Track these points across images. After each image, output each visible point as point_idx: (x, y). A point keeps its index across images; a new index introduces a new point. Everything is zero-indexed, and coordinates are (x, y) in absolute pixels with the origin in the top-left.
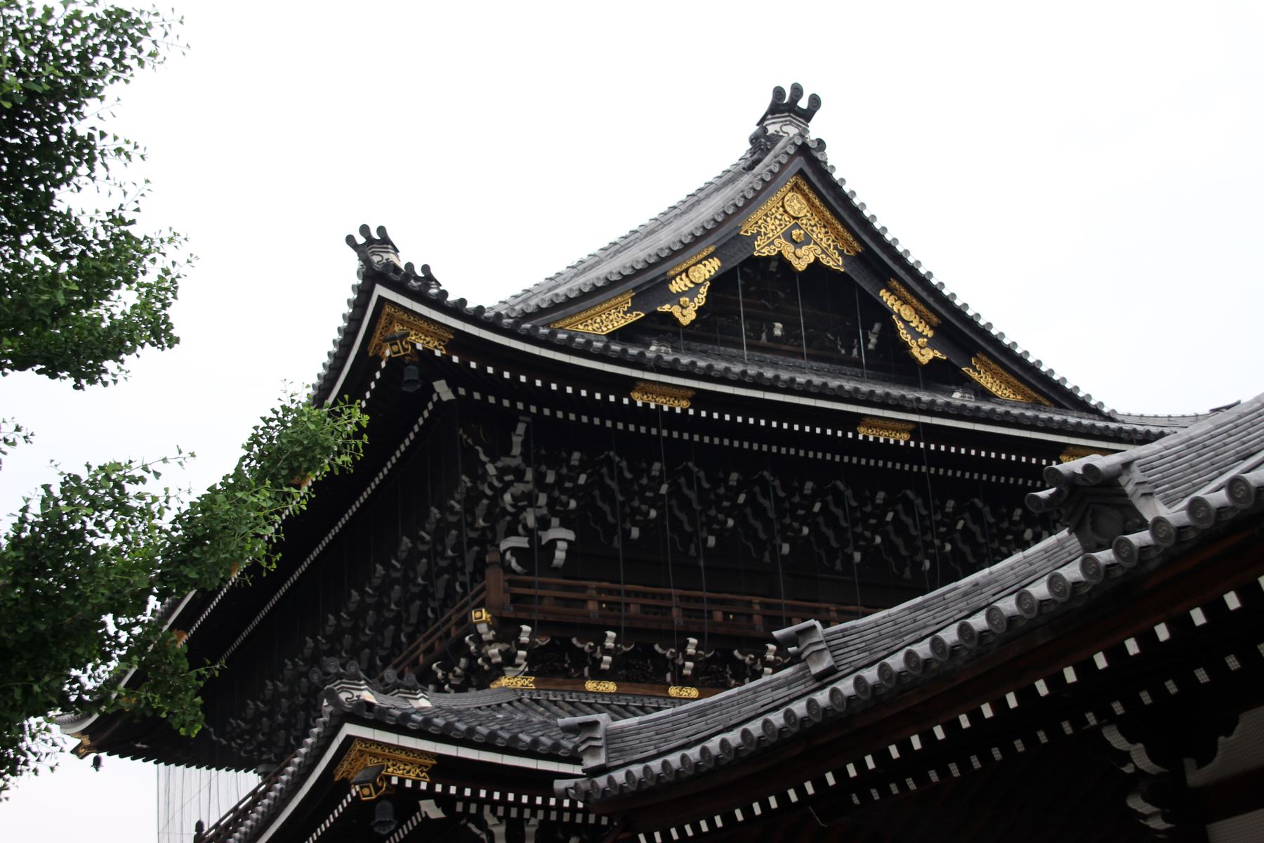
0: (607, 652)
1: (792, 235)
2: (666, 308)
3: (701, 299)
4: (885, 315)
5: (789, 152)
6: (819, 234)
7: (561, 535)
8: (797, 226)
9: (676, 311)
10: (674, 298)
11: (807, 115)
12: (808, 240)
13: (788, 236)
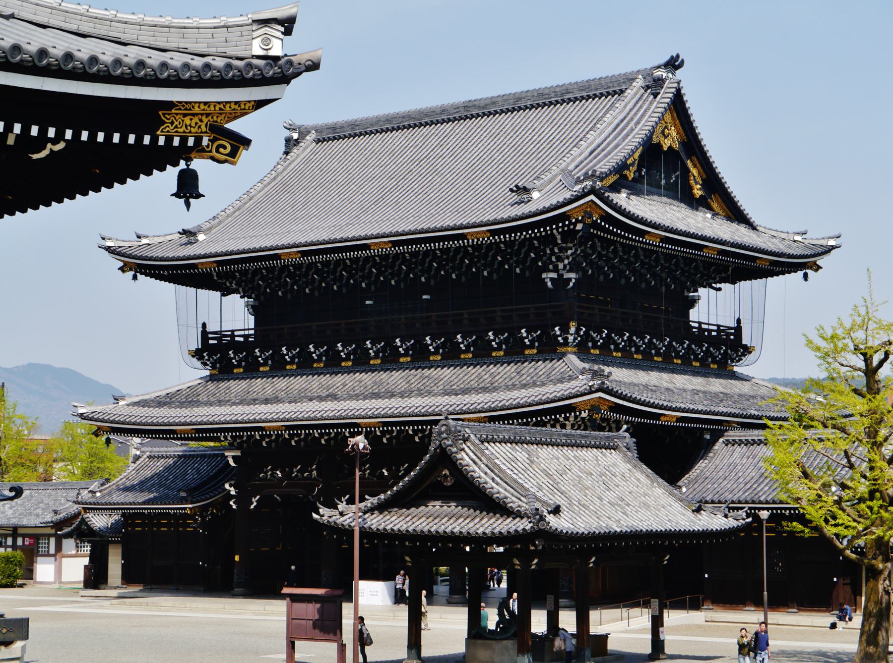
4: (686, 172)
6: (673, 132)
8: (666, 127)
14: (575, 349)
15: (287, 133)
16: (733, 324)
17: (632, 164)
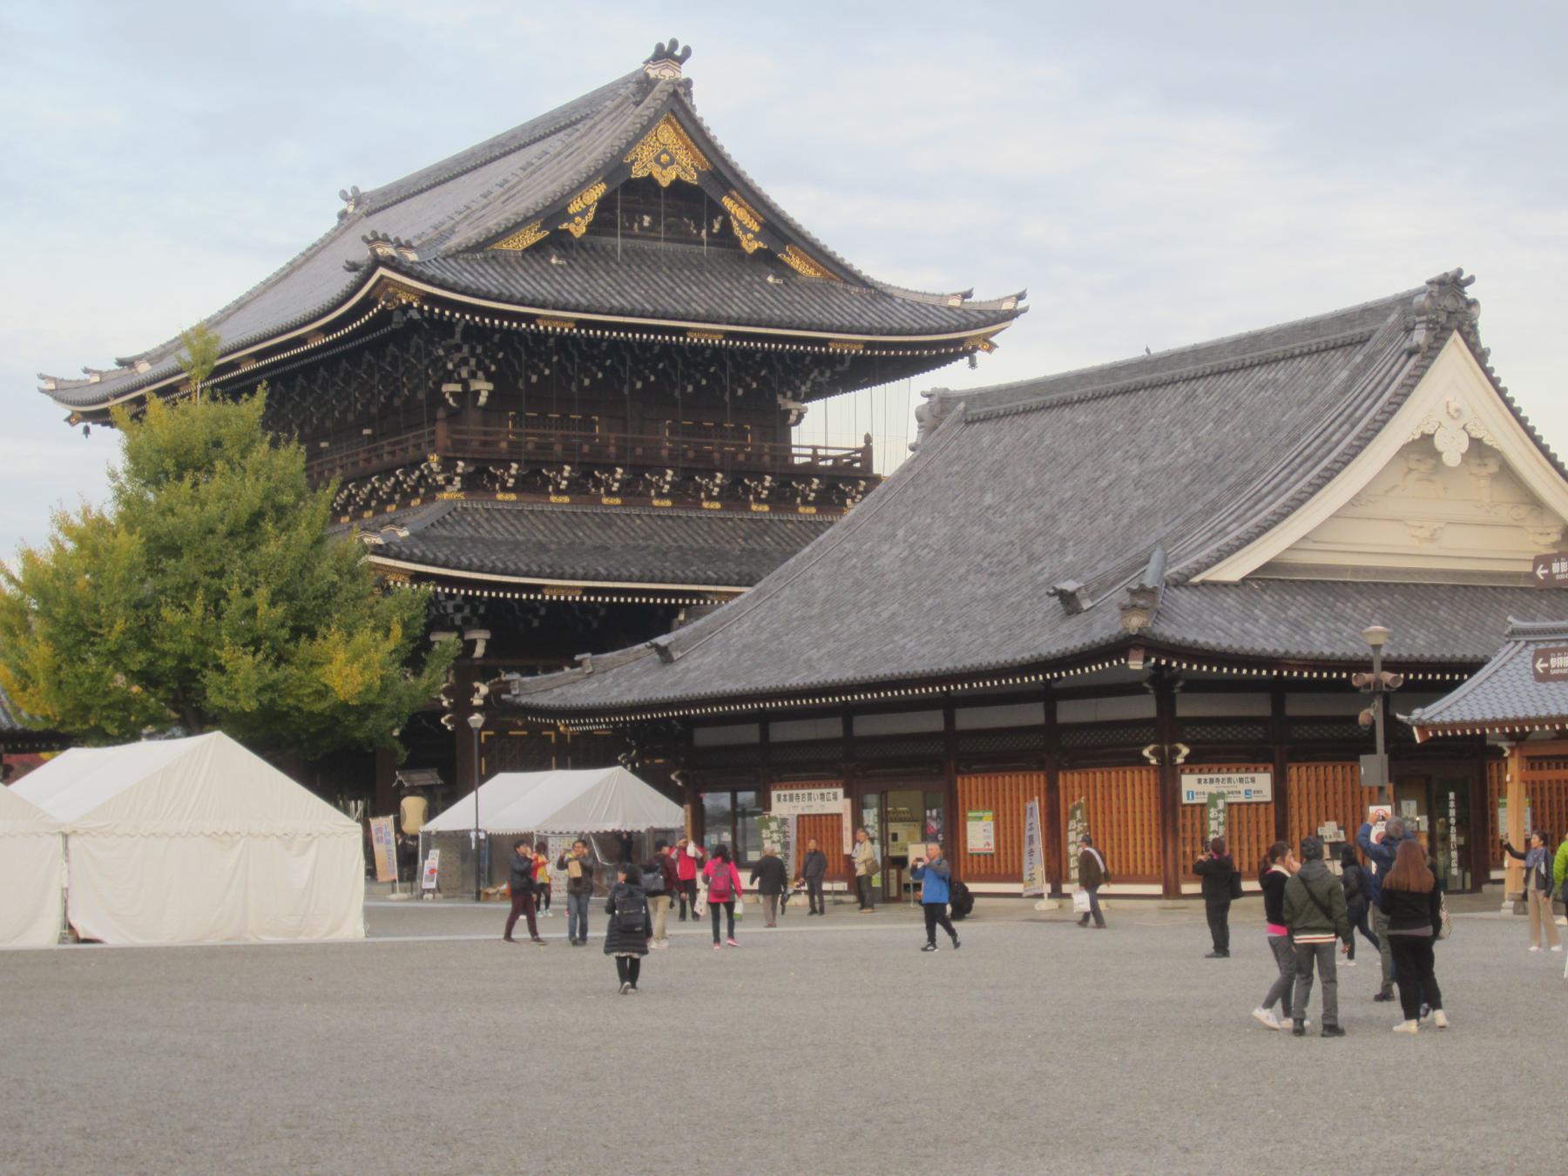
0: (511, 476)
1: (665, 161)
2: (565, 226)
3: (590, 216)
4: (726, 214)
5: (664, 99)
6: (683, 157)
7: (483, 387)
8: (665, 151)
9: (572, 227)
10: (570, 218)
11: (681, 60)
12: (672, 161)
13: (657, 160)
14: (329, 493)
15: (343, 205)
16: (861, 444)
17: (583, 214)
